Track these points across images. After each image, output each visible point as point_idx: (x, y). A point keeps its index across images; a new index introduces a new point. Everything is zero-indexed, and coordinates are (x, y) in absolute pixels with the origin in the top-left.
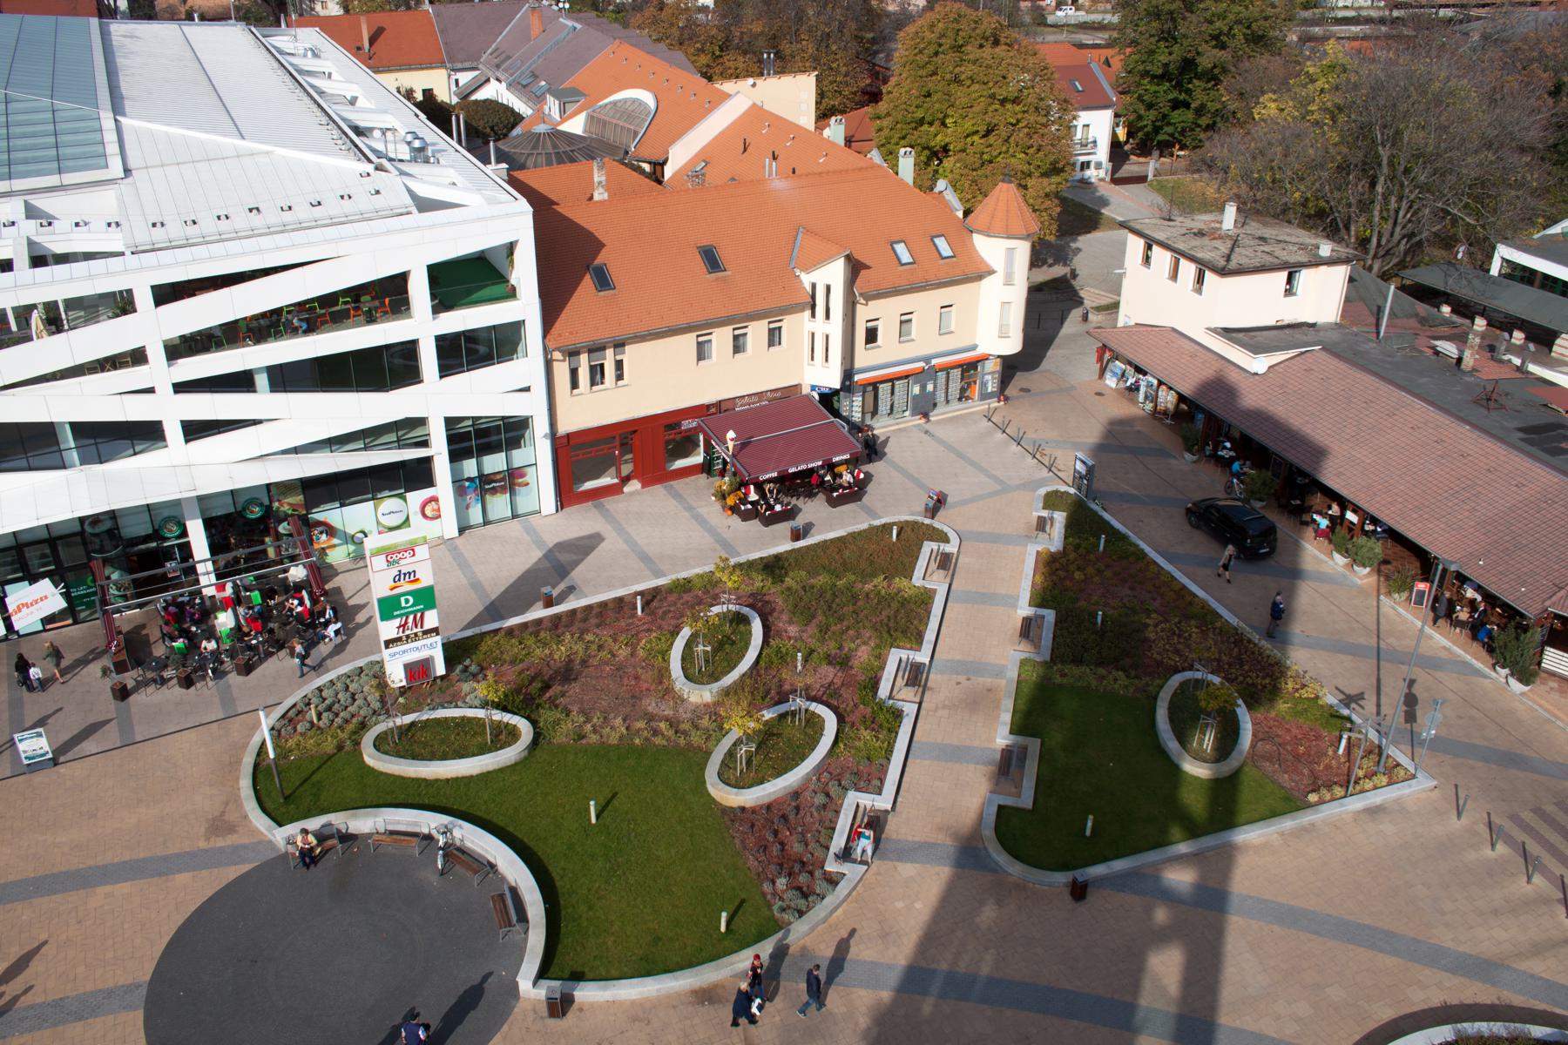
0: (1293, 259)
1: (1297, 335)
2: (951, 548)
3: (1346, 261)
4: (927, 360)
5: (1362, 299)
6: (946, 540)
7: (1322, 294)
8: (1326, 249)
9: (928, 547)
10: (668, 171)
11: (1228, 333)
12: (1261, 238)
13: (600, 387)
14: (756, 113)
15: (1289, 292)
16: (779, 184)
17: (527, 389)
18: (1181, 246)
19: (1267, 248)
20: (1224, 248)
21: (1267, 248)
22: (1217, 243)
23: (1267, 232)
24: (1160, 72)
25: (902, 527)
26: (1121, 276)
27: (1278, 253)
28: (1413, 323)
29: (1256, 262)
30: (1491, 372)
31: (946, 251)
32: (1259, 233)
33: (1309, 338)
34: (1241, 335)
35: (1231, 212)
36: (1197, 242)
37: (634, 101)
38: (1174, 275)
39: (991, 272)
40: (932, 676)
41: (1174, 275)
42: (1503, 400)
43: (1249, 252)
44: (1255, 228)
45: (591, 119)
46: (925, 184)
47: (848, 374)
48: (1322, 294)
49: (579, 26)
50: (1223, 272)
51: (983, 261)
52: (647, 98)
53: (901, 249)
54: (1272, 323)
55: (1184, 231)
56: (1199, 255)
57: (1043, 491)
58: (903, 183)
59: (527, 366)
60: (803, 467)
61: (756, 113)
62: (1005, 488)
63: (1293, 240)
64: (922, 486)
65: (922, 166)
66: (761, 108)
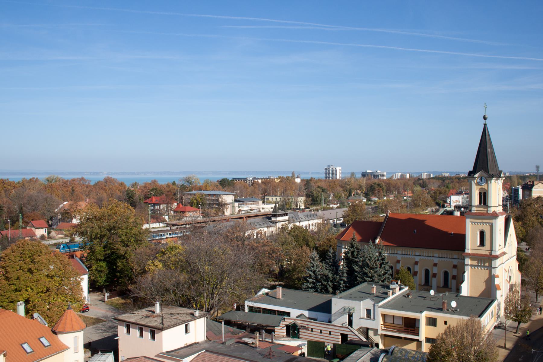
0: (186, 319)
1: (194, 348)
3: (204, 316)
5: (211, 330)
7: (198, 330)
8: (197, 313)
11: (158, 356)
12: (171, 314)
15: (187, 331)
18: (142, 323)
19: (175, 317)
20: (159, 320)
21: (175, 317)
22: (156, 319)
23: (172, 311)
24: (103, 258)
27: (180, 318)
28: (230, 335)
29: (173, 323)
30: (265, 346)
31: (46, 343)
32: (169, 313)
33: (198, 349)
34: (173, 353)
35: (158, 305)
36: (148, 320)
38: (141, 335)
39: (67, 348)
41: (141, 335)
42: (274, 354)
43: (169, 320)
44: (166, 310)
48: (198, 330)
51: (64, 345)
53: (26, 346)
54: (183, 345)
55: (141, 317)
56: (151, 325)
63: (182, 312)
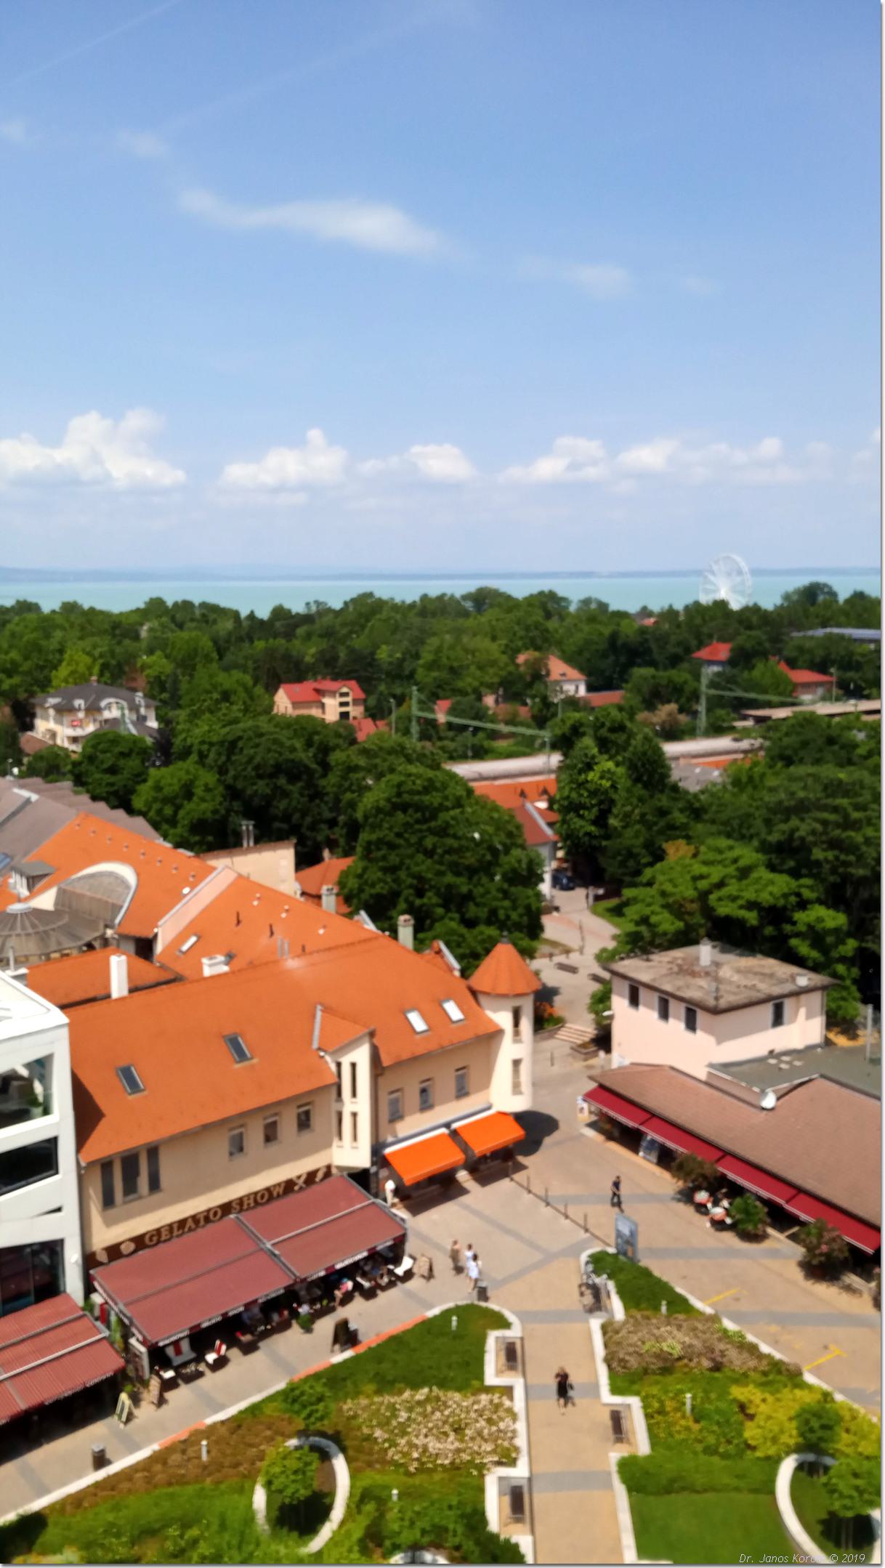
0: (777, 990)
2: (514, 1333)
4: (447, 1125)
6: (506, 1325)
9: (493, 1340)
10: (159, 948)
13: (131, 1197)
14: (243, 884)
16: (292, 964)
17: (59, 1210)
18: (668, 987)
25: (457, 1310)
26: (611, 1017)
37: (111, 874)
40: (536, 1501)
45: (62, 894)
46: (420, 944)
47: (377, 1150)
49: (34, 797)
50: (716, 1011)
52: (127, 873)
56: (688, 994)
57: (584, 1257)
58: (404, 948)
59: (60, 1187)
60: (347, 1262)
61: (243, 884)
62: (549, 1257)
64: (506, 1281)
65: (418, 929)
66: (247, 879)
